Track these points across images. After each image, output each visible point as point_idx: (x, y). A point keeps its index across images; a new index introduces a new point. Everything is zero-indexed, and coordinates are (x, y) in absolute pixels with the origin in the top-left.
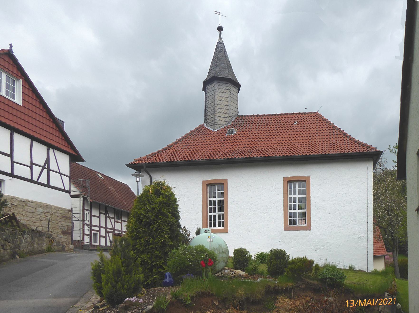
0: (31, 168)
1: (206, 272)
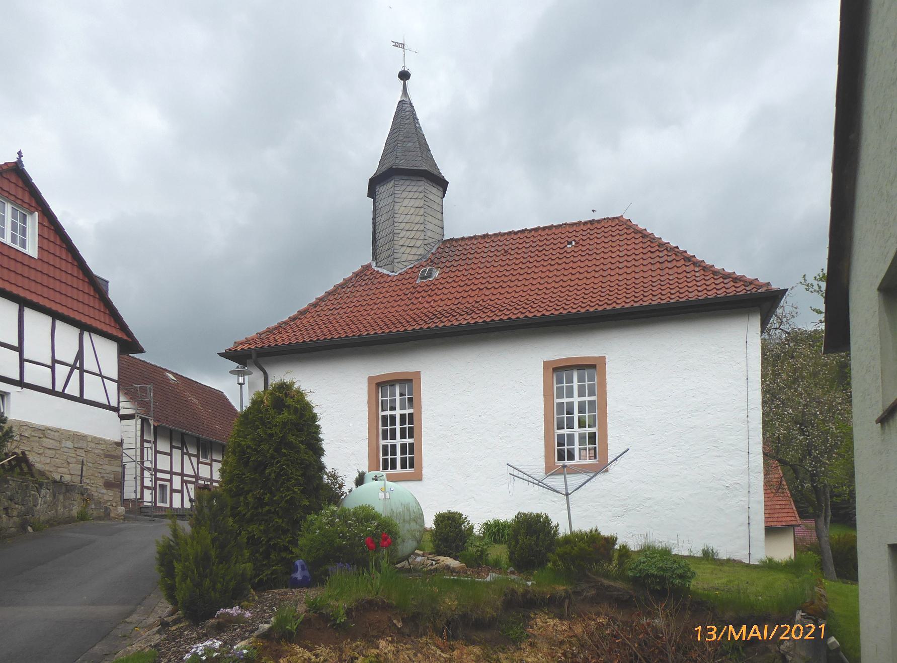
0: (53, 368)
1: (376, 560)
